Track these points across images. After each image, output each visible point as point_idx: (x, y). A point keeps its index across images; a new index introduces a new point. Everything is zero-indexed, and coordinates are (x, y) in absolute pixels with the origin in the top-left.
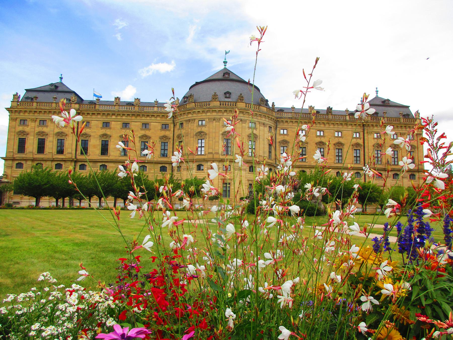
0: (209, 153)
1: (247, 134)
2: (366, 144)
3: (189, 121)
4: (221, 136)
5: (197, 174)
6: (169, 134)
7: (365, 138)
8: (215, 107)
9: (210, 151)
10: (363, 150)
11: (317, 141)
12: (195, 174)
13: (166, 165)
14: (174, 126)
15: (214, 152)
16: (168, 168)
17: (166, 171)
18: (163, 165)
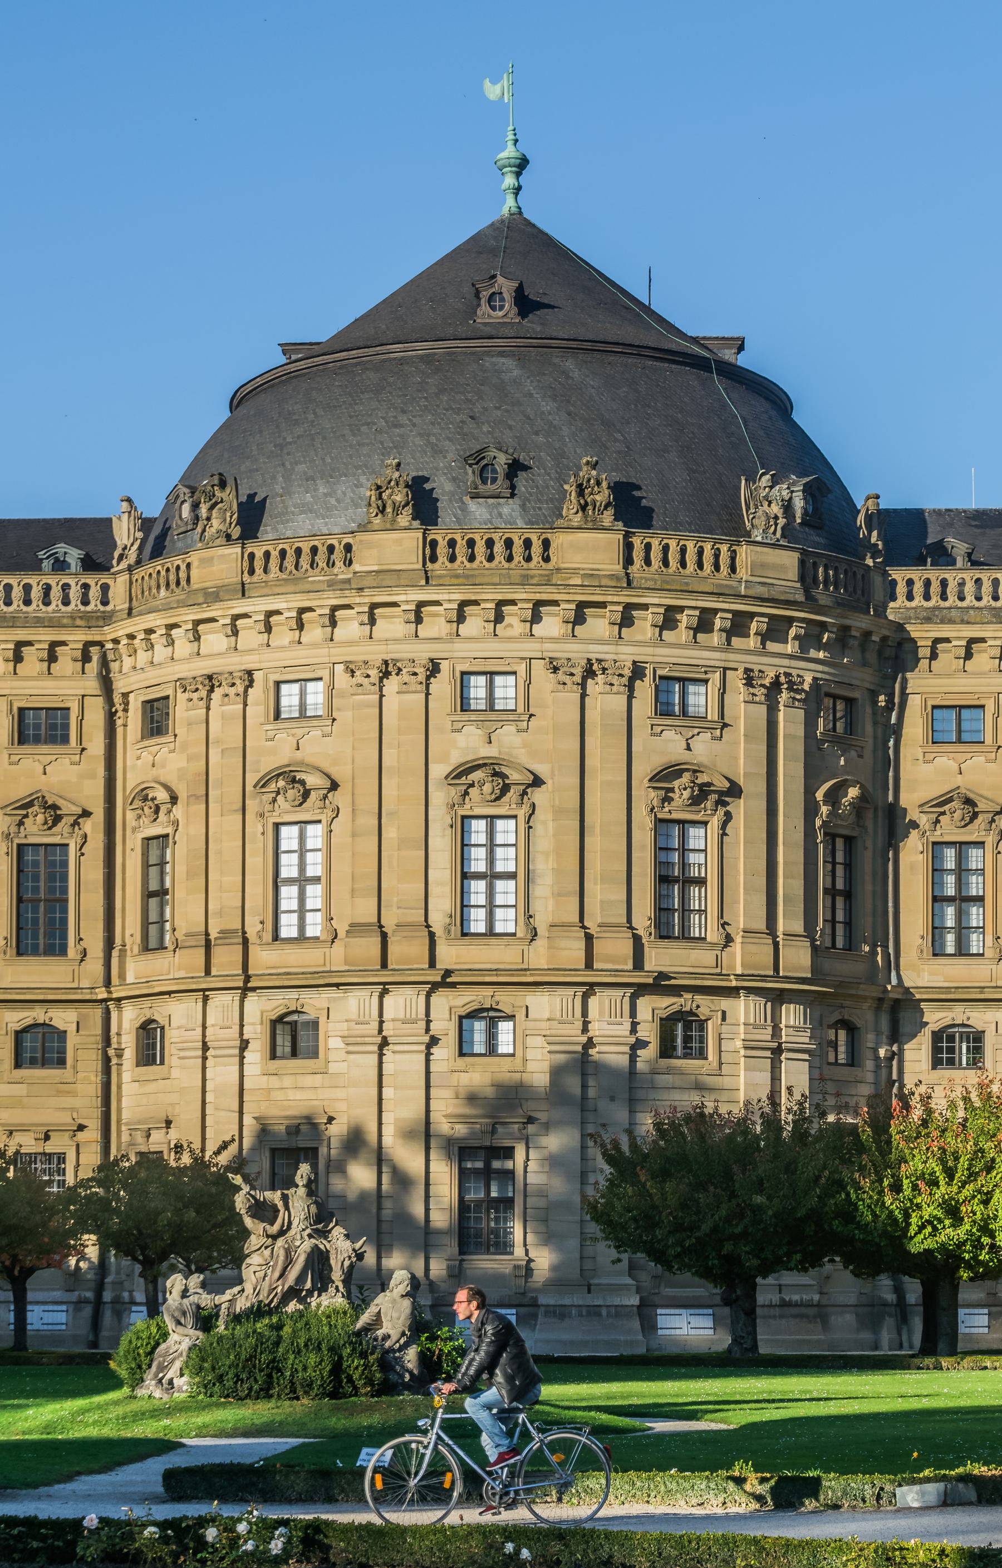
0: (356, 929)
1: (642, 770)
3: (211, 681)
4: (439, 797)
5: (274, 1082)
6: (69, 775)
9: (366, 911)
12: (264, 1082)
13: (63, 1019)
15: (389, 922)
16: (72, 1041)
17: (61, 1062)
18: (38, 1015)
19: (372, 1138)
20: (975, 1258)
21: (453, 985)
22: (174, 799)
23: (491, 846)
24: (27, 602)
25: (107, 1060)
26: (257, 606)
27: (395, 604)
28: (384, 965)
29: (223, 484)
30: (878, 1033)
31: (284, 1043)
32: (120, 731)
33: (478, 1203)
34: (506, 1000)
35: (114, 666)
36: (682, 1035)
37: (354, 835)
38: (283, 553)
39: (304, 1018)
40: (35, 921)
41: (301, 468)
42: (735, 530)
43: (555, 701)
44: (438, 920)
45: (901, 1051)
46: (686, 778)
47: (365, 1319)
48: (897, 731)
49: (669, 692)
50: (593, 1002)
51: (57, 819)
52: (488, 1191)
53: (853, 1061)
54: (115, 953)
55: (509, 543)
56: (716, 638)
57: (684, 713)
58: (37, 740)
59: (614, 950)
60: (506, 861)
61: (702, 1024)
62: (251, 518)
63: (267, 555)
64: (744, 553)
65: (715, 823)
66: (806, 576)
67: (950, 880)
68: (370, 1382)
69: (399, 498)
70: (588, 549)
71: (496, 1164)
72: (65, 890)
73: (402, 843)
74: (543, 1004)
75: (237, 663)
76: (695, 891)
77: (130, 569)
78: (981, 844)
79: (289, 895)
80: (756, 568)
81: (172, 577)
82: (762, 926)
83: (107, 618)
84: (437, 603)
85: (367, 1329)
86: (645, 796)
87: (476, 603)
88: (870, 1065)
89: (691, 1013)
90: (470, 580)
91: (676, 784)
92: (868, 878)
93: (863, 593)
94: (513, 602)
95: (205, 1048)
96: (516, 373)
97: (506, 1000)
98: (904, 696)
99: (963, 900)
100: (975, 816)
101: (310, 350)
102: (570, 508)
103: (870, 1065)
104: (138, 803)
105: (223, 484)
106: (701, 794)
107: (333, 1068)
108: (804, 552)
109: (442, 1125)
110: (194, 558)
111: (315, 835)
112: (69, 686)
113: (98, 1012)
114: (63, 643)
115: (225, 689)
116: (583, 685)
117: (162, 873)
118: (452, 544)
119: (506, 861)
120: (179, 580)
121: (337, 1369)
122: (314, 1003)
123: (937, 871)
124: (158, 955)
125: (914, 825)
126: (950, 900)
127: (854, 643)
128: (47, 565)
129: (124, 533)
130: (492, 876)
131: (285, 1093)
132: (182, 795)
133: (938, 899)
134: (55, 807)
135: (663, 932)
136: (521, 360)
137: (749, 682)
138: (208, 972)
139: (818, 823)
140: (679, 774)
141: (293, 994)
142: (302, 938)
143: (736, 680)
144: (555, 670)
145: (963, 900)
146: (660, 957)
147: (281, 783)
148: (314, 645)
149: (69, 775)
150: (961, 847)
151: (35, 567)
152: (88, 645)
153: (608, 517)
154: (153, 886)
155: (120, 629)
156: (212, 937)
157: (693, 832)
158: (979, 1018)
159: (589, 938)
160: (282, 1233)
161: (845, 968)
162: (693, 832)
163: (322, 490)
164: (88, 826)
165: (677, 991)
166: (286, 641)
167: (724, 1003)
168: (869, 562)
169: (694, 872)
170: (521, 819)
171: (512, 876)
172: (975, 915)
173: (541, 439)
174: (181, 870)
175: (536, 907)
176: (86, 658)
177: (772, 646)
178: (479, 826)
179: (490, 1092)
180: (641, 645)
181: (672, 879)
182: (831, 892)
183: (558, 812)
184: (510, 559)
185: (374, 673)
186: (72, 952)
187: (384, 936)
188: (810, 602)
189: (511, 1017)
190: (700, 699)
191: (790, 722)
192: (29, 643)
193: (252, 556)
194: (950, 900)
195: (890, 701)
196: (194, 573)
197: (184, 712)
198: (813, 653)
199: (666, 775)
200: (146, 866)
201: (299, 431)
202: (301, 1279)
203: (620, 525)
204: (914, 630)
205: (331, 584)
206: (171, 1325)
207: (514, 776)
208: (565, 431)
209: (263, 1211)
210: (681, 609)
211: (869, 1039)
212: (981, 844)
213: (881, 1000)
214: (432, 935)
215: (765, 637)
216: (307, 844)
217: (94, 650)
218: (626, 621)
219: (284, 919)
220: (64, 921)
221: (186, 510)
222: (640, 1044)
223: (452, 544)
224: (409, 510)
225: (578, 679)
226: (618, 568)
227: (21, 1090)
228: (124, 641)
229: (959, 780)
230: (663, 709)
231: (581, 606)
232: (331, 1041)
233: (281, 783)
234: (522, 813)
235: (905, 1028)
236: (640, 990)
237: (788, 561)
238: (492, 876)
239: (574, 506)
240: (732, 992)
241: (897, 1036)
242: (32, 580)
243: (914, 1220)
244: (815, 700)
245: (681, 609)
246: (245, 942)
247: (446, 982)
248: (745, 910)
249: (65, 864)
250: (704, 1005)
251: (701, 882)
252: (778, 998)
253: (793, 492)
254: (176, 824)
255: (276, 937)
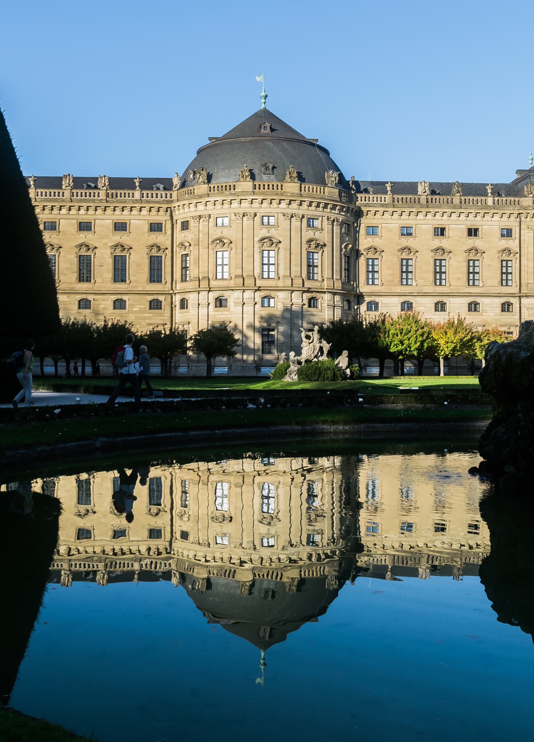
0: (236, 276)
1: (304, 240)
2: (522, 249)
3: (200, 217)
4: (257, 245)
5: (216, 313)
6: (163, 239)
7: (522, 238)
8: (244, 193)
9: (239, 272)
10: (518, 260)
11: (434, 247)
13: (161, 298)
14: (173, 225)
17: (161, 308)
18: (155, 297)
19: (240, 327)
20: (405, 353)
21: (260, 290)
22: (190, 245)
23: (269, 257)
24: (152, 197)
25: (172, 308)
26: (212, 199)
27: (246, 199)
28: (244, 285)
29: (203, 170)
30: (355, 303)
31: (218, 303)
32: (175, 229)
33: (266, 342)
34: (273, 294)
35: (173, 213)
36: (312, 302)
37: (236, 254)
38: (218, 187)
39: (223, 298)
40: (154, 274)
41: (221, 166)
42: (324, 184)
43: (284, 223)
44: (256, 275)
45: (359, 307)
46: (314, 242)
47: (336, 362)
48: (359, 232)
49: (310, 221)
50: (293, 294)
51: (160, 250)
52: (268, 339)
53: (349, 309)
54: (174, 282)
55: (273, 185)
56: (321, 209)
57: (313, 226)
58: (154, 231)
59: (298, 282)
60: (272, 261)
61: (317, 300)
62: (209, 178)
63: (214, 187)
64: (326, 189)
65: (320, 252)
66: (340, 195)
67: (370, 267)
68: (341, 377)
69: (247, 174)
70: (292, 187)
71: (271, 333)
72: (161, 267)
73: (248, 256)
74: (281, 295)
75: (207, 213)
76: (315, 268)
77: (178, 190)
78: (378, 259)
79: (219, 268)
80: (330, 193)
81: (189, 192)
82: (331, 277)
83: (172, 202)
84: (257, 199)
85: (337, 365)
86: (305, 246)
87: (266, 199)
88: (353, 310)
89: (315, 297)
90: (263, 194)
91: (312, 243)
92: (352, 266)
93: (352, 199)
94: (274, 199)
95: (199, 305)
96: (272, 145)
97: (273, 294)
98: (360, 224)
99: (373, 272)
100: (376, 252)
101: (217, 139)
102: (287, 178)
103: (353, 310)
104: (180, 246)
105: (203, 170)
106: (317, 245)
107: (231, 310)
108: (340, 190)
109: (257, 324)
110: (195, 187)
111: (226, 254)
112: (162, 218)
113: (170, 296)
114: (161, 207)
115: (204, 219)
116: (291, 219)
117: (186, 263)
118: (260, 185)
119: (272, 261)
120: (191, 193)
121: (334, 374)
122: (226, 294)
123: (368, 265)
124: (186, 282)
125: (362, 254)
126: (371, 272)
127: (350, 211)
128: (155, 189)
129: (176, 181)
130: (269, 264)
131: (218, 316)
132: (192, 244)
133: (368, 272)
134: (159, 247)
135: (309, 278)
136: (273, 142)
137: (328, 220)
138: (199, 287)
139: (343, 253)
140: (312, 241)
141: (221, 292)
142: (223, 279)
143: (325, 219)
144: (284, 216)
145: (373, 272)
146: (308, 284)
147: (218, 241)
148: (226, 209)
149: (163, 239)
150: (373, 259)
151: (152, 189)
152: (167, 208)
153: (296, 180)
154: (184, 266)
155: (176, 204)
156: (200, 278)
157: (315, 254)
158: (377, 299)
159: (292, 279)
160: (312, 342)
161: (348, 287)
162: (315, 254)
163: (227, 172)
164: (167, 251)
165: (312, 292)
166: (219, 208)
167: (323, 295)
168: (353, 192)
169: (315, 264)
170: (276, 251)
171: (274, 264)
172: (376, 275)
173: (279, 161)
174: (192, 262)
175: (280, 272)
176: (167, 211)
177: (333, 211)
178: (266, 253)
179: (266, 316)
180: (304, 210)
181: (311, 266)
182: (345, 269)
183: (285, 250)
184: (273, 189)
185: (241, 216)
186: (163, 282)
187: (244, 278)
188: (341, 201)
189: (274, 298)
190: (317, 223)
191: (337, 229)
192: (153, 207)
193: (210, 187)
194: (371, 272)
195: (357, 225)
196: (195, 191)
197: (192, 224)
198: (341, 213)
199: (310, 241)
200: (182, 261)
201: (220, 158)
202: (318, 353)
203: (299, 182)
204: (363, 209)
205: (230, 194)
206: (291, 364)
207: (274, 241)
208: (285, 159)
209: (308, 337)
210: (313, 202)
211: (353, 304)
212: (378, 259)
213: (355, 295)
214: (255, 278)
215: (331, 209)
216: (224, 257)
217: (169, 209)
218: (301, 204)
219: (218, 274)
220: (161, 274)
221: (191, 176)
222: (304, 304)
223: (260, 185)
224: (249, 177)
225: (289, 218)
226: (299, 192)
227: (151, 315)
228: (177, 207)
229: (373, 244)
230: (309, 226)
231: (291, 200)
232: (231, 303)
233: (218, 241)
234: (276, 249)
235: (361, 302)
236: (304, 292)
237: (336, 191)
238: (269, 264)
239: (289, 177)
240: (325, 292)
241: (359, 303)
242: (153, 192)
243: (392, 344)
244: (342, 224)
245: (313, 202)
246: (209, 280)
247: (259, 289)
248: (327, 274)
249: (161, 260)
250: (318, 295)
251: (317, 266)
252: (335, 294)
253: (336, 174)
254: (191, 251)
255: (216, 278)
